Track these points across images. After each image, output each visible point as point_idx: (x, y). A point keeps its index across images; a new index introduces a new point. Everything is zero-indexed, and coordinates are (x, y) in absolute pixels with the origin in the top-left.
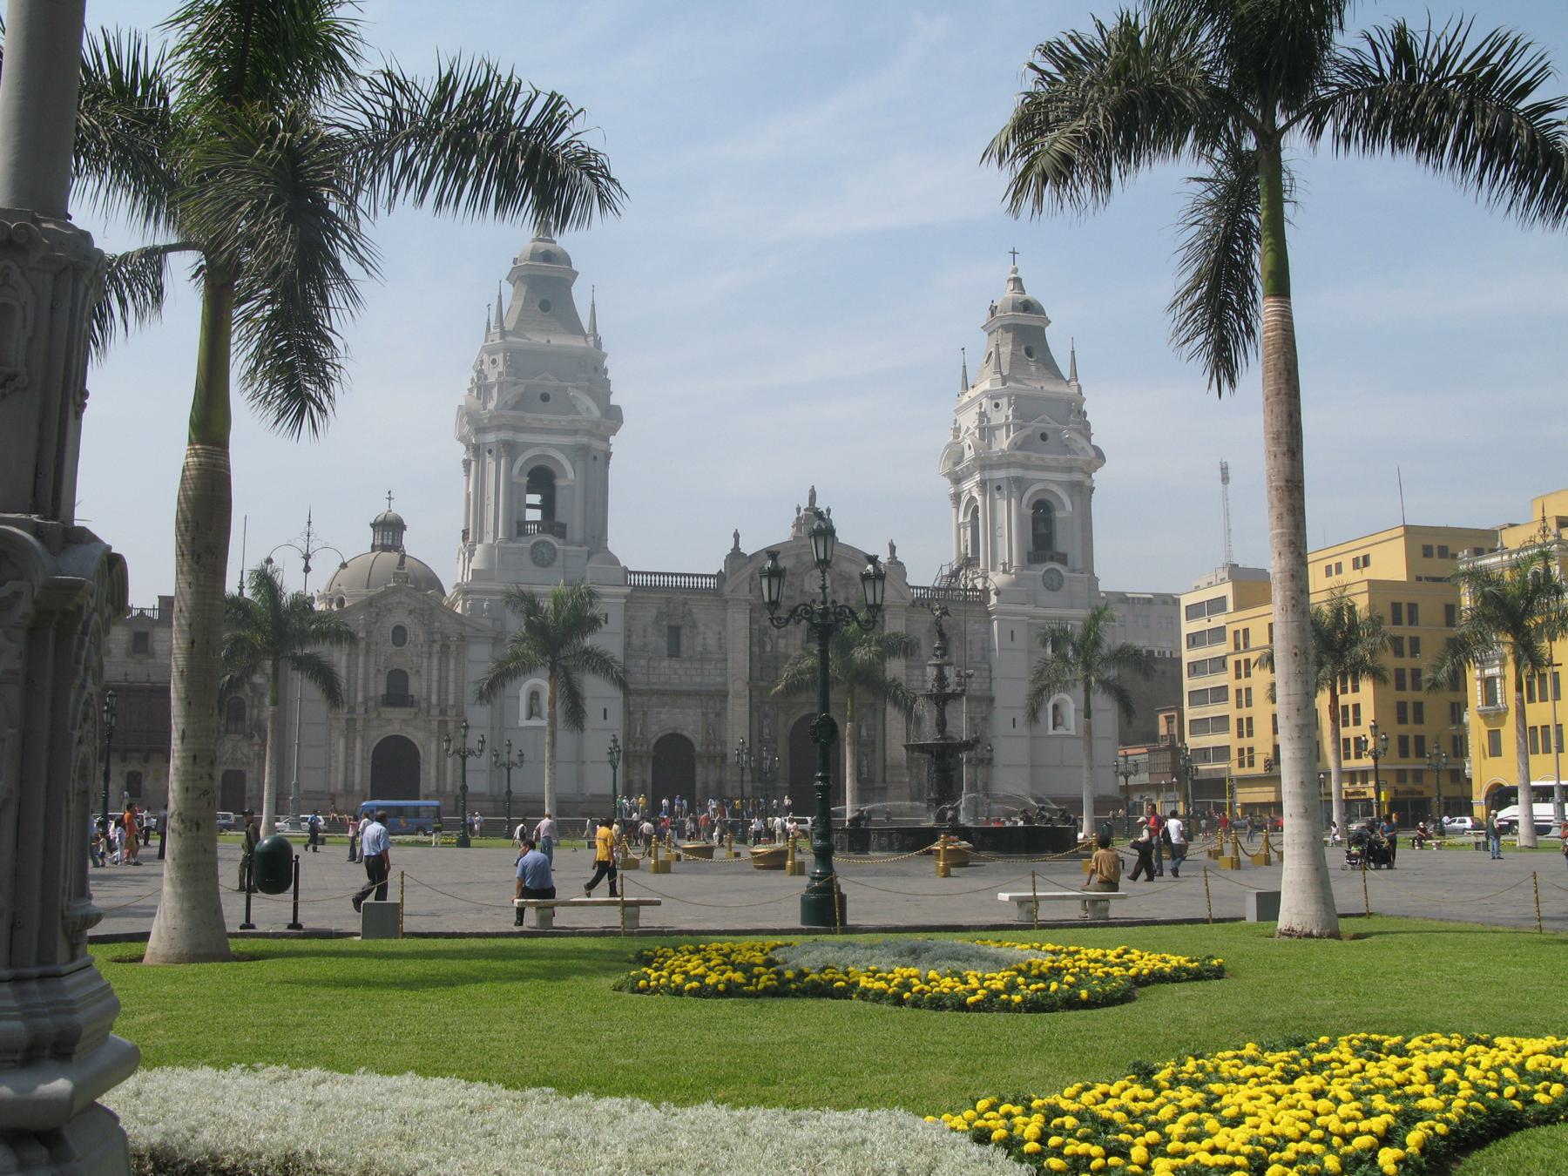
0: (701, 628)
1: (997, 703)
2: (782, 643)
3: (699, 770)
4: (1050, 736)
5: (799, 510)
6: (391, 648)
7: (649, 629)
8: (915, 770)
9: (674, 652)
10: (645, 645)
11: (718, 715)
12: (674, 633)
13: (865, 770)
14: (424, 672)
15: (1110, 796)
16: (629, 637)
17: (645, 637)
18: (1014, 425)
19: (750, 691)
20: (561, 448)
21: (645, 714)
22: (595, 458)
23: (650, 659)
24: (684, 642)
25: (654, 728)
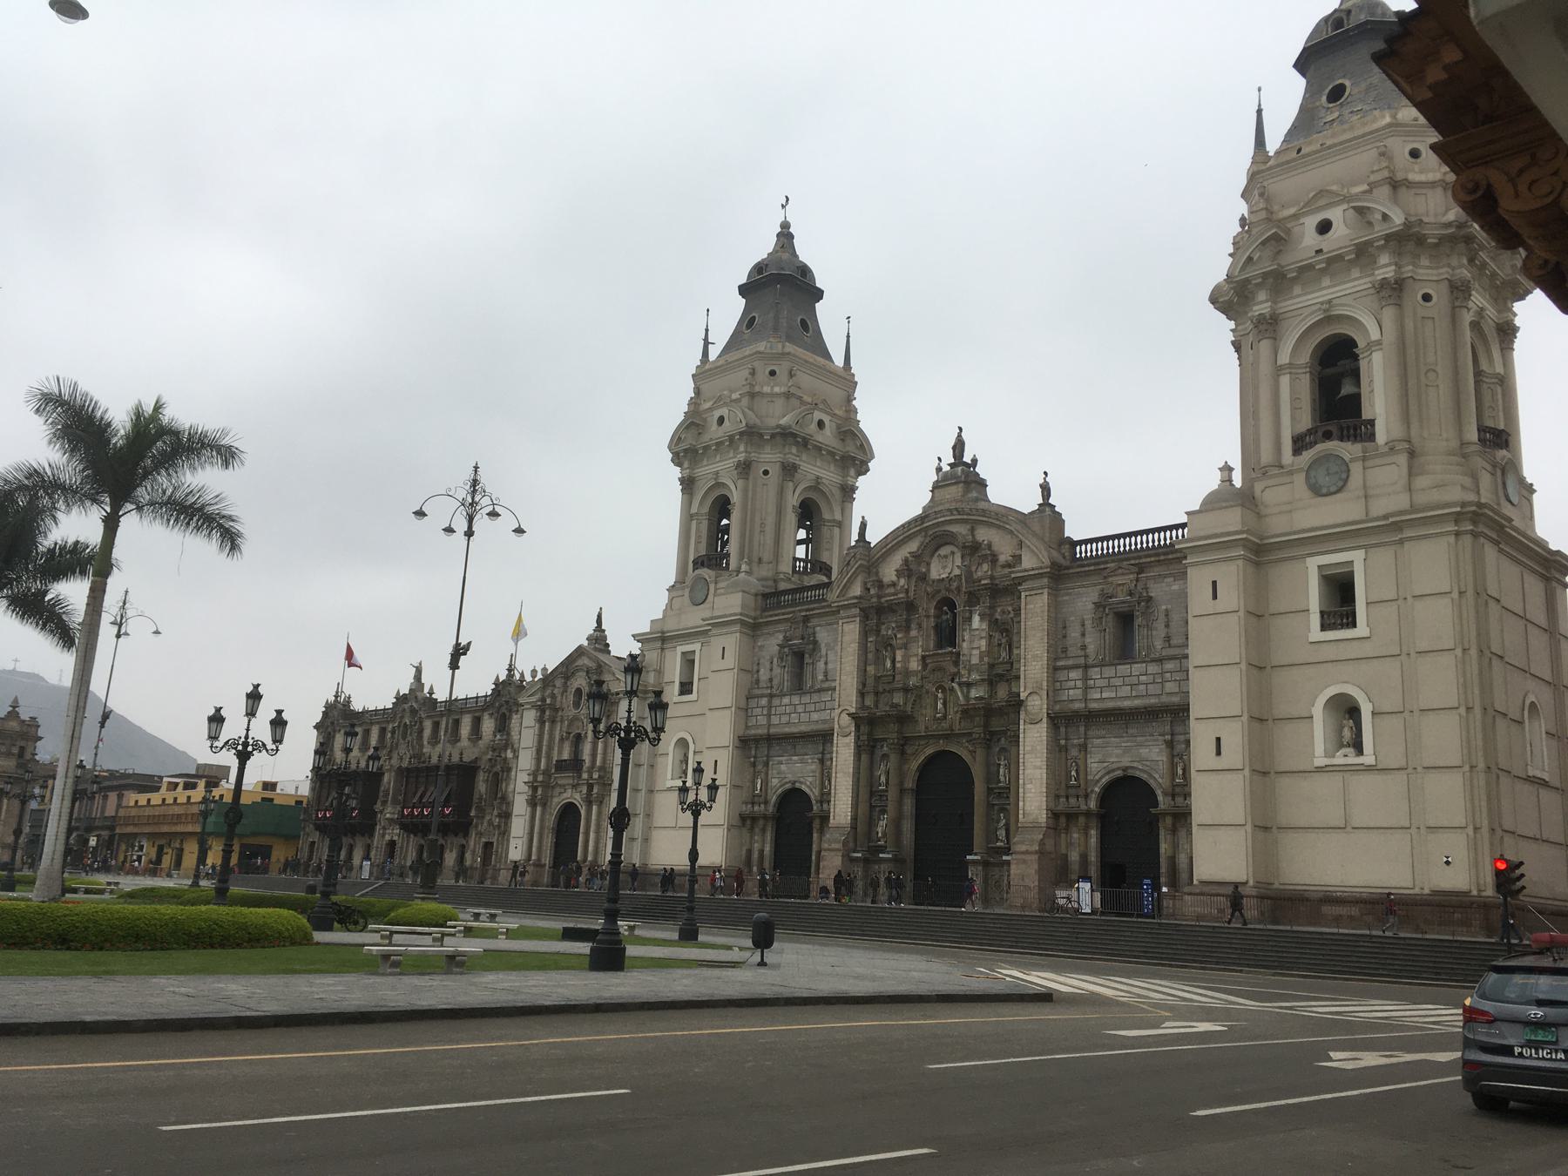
0: (823, 652)
1: (1194, 712)
2: (899, 655)
4: (1320, 770)
5: (939, 469)
6: (572, 712)
7: (775, 660)
8: (1075, 835)
9: (798, 686)
10: (771, 680)
12: (799, 656)
13: (1002, 833)
15: (1467, 894)
16: (758, 671)
17: (771, 670)
19: (858, 727)
21: (766, 764)
22: (766, 473)
23: (771, 696)
24: (808, 670)
25: (775, 782)
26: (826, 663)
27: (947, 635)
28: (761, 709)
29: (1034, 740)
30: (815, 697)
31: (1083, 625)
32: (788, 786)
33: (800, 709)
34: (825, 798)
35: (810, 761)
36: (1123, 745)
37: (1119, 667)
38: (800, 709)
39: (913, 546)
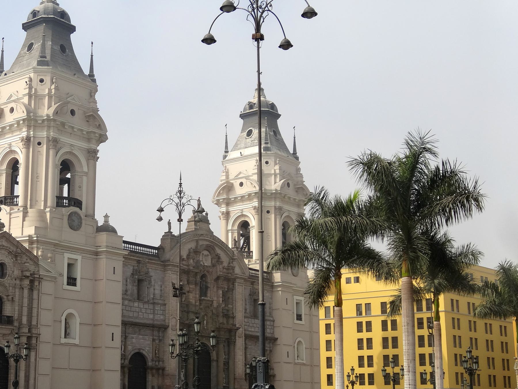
3: (149, 378)
7: (128, 280)
9: (139, 298)
11: (160, 341)
14: (17, 299)
18: (280, 175)
20: (80, 149)
25: (130, 348)
26: (154, 289)
27: (204, 291)
28: (125, 306)
29: (240, 342)
30: (151, 306)
31: (246, 301)
32: (136, 351)
33: (144, 311)
34: (158, 358)
35: (147, 339)
36: (255, 349)
37: (255, 320)
38: (144, 311)
39: (193, 245)
